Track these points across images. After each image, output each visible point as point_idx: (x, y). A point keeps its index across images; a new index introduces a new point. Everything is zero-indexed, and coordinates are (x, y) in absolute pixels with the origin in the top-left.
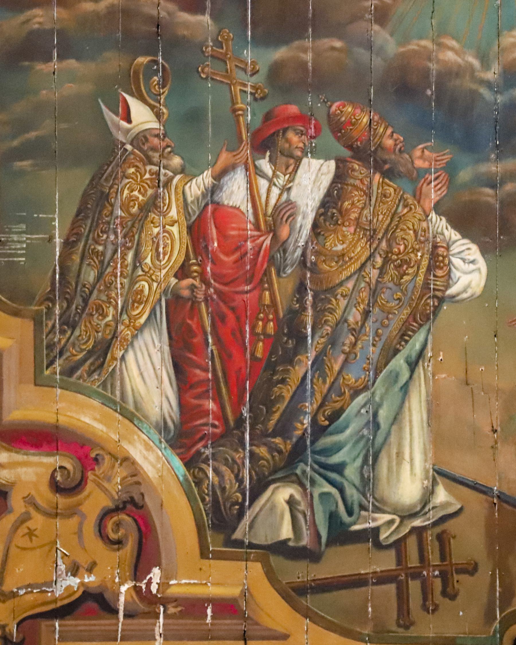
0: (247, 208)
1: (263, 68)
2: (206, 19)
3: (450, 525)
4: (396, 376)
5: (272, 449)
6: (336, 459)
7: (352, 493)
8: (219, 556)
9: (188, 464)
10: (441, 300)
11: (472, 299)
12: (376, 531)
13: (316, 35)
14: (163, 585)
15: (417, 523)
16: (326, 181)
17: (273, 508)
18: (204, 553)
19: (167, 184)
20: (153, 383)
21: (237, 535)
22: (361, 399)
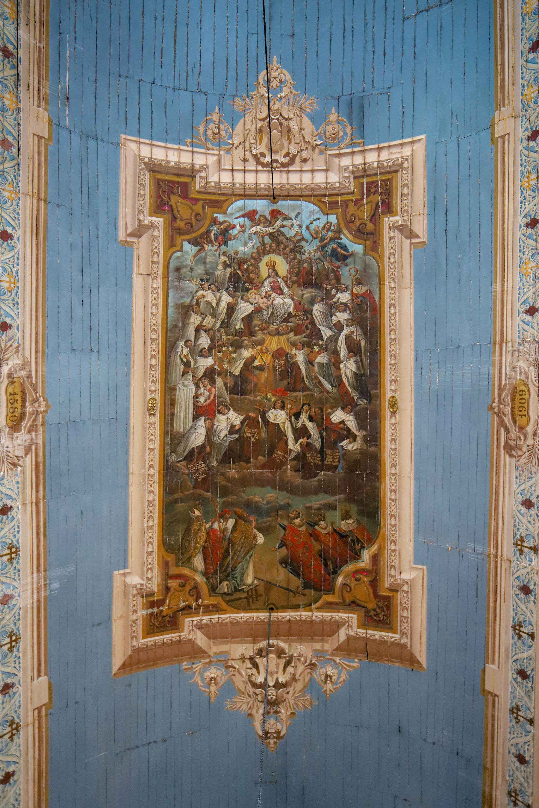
0: (218, 529)
1: (221, 502)
2: (210, 493)
3: (257, 587)
4: (247, 560)
5: (223, 575)
6: (235, 576)
7: (239, 582)
8: (214, 596)
9: (207, 579)
10: (255, 545)
11: (261, 545)
12: (243, 589)
13: (231, 495)
14: (202, 603)
15: (251, 587)
16: (233, 523)
17: (223, 586)
18: (210, 595)
19: (202, 525)
20: (199, 564)
21: (217, 591)
22: (240, 564)
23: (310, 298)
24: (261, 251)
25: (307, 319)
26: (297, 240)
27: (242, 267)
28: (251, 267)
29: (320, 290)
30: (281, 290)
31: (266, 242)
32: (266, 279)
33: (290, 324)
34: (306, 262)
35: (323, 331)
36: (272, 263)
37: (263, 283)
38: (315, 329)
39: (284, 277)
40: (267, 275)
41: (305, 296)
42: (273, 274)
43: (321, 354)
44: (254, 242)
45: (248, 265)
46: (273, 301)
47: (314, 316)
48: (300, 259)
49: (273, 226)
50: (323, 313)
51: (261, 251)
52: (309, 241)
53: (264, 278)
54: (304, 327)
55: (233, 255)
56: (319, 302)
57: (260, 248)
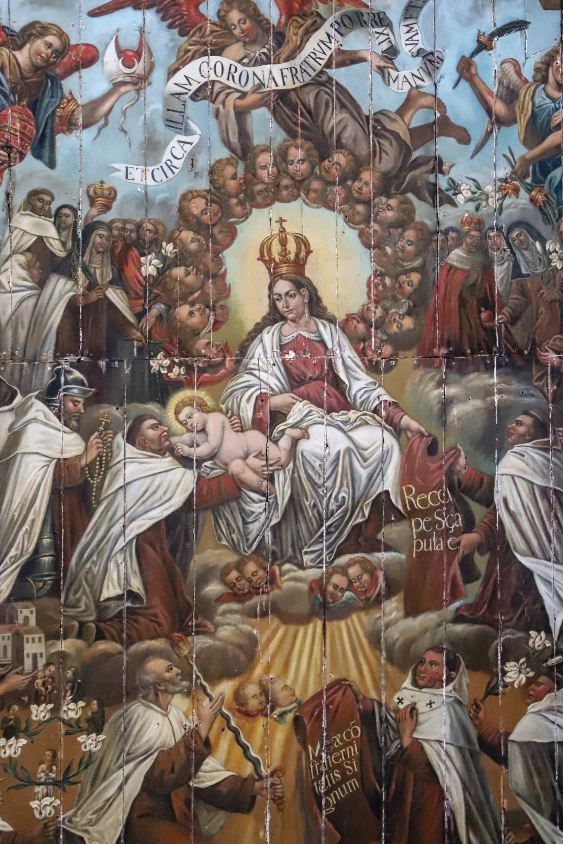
23: (479, 423)
24: (232, 184)
25: (469, 526)
26: (412, 132)
27: (130, 270)
28: (179, 272)
29: (528, 380)
30: (337, 382)
31: (258, 140)
32: (258, 329)
33: (383, 556)
34: (458, 245)
35: (547, 582)
36: (292, 246)
37: (244, 349)
38: (505, 575)
39: (350, 317)
40: (264, 309)
41: (456, 411)
42: (293, 302)
43: (539, 698)
44: (195, 139)
45: (164, 259)
46: (295, 442)
47: (502, 512)
48: (429, 223)
49: (290, 57)
50: (544, 491)
51: (232, 184)
52: (476, 136)
53: (250, 326)
54: (456, 569)
55: (84, 209)
56: (522, 439)
57: (229, 171)
